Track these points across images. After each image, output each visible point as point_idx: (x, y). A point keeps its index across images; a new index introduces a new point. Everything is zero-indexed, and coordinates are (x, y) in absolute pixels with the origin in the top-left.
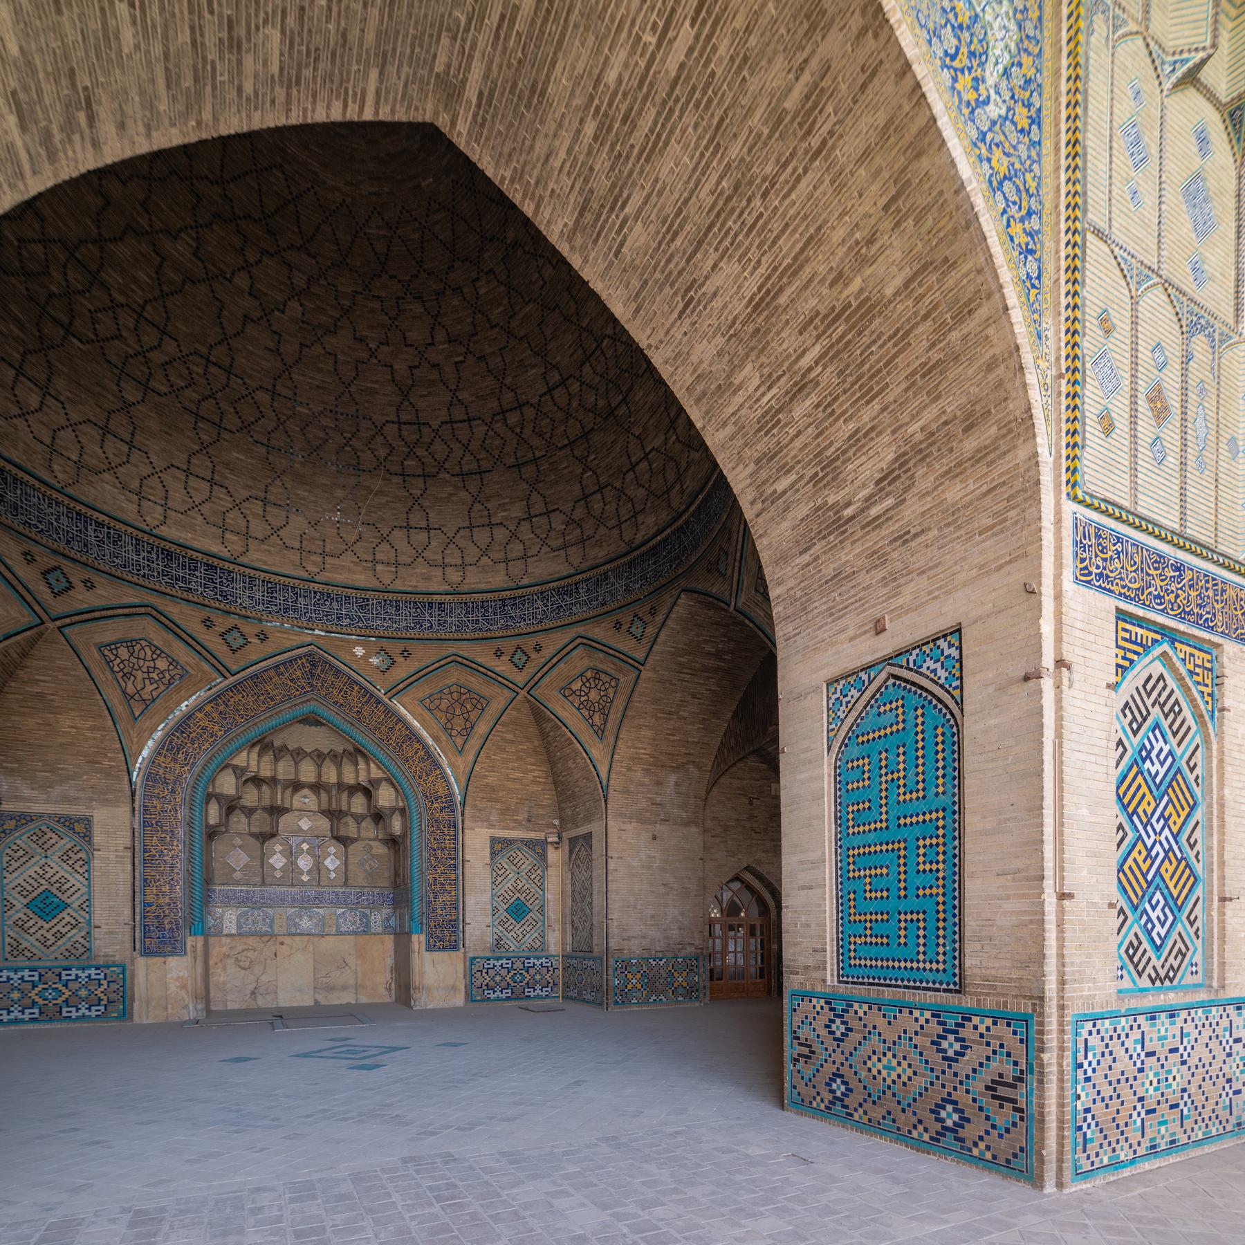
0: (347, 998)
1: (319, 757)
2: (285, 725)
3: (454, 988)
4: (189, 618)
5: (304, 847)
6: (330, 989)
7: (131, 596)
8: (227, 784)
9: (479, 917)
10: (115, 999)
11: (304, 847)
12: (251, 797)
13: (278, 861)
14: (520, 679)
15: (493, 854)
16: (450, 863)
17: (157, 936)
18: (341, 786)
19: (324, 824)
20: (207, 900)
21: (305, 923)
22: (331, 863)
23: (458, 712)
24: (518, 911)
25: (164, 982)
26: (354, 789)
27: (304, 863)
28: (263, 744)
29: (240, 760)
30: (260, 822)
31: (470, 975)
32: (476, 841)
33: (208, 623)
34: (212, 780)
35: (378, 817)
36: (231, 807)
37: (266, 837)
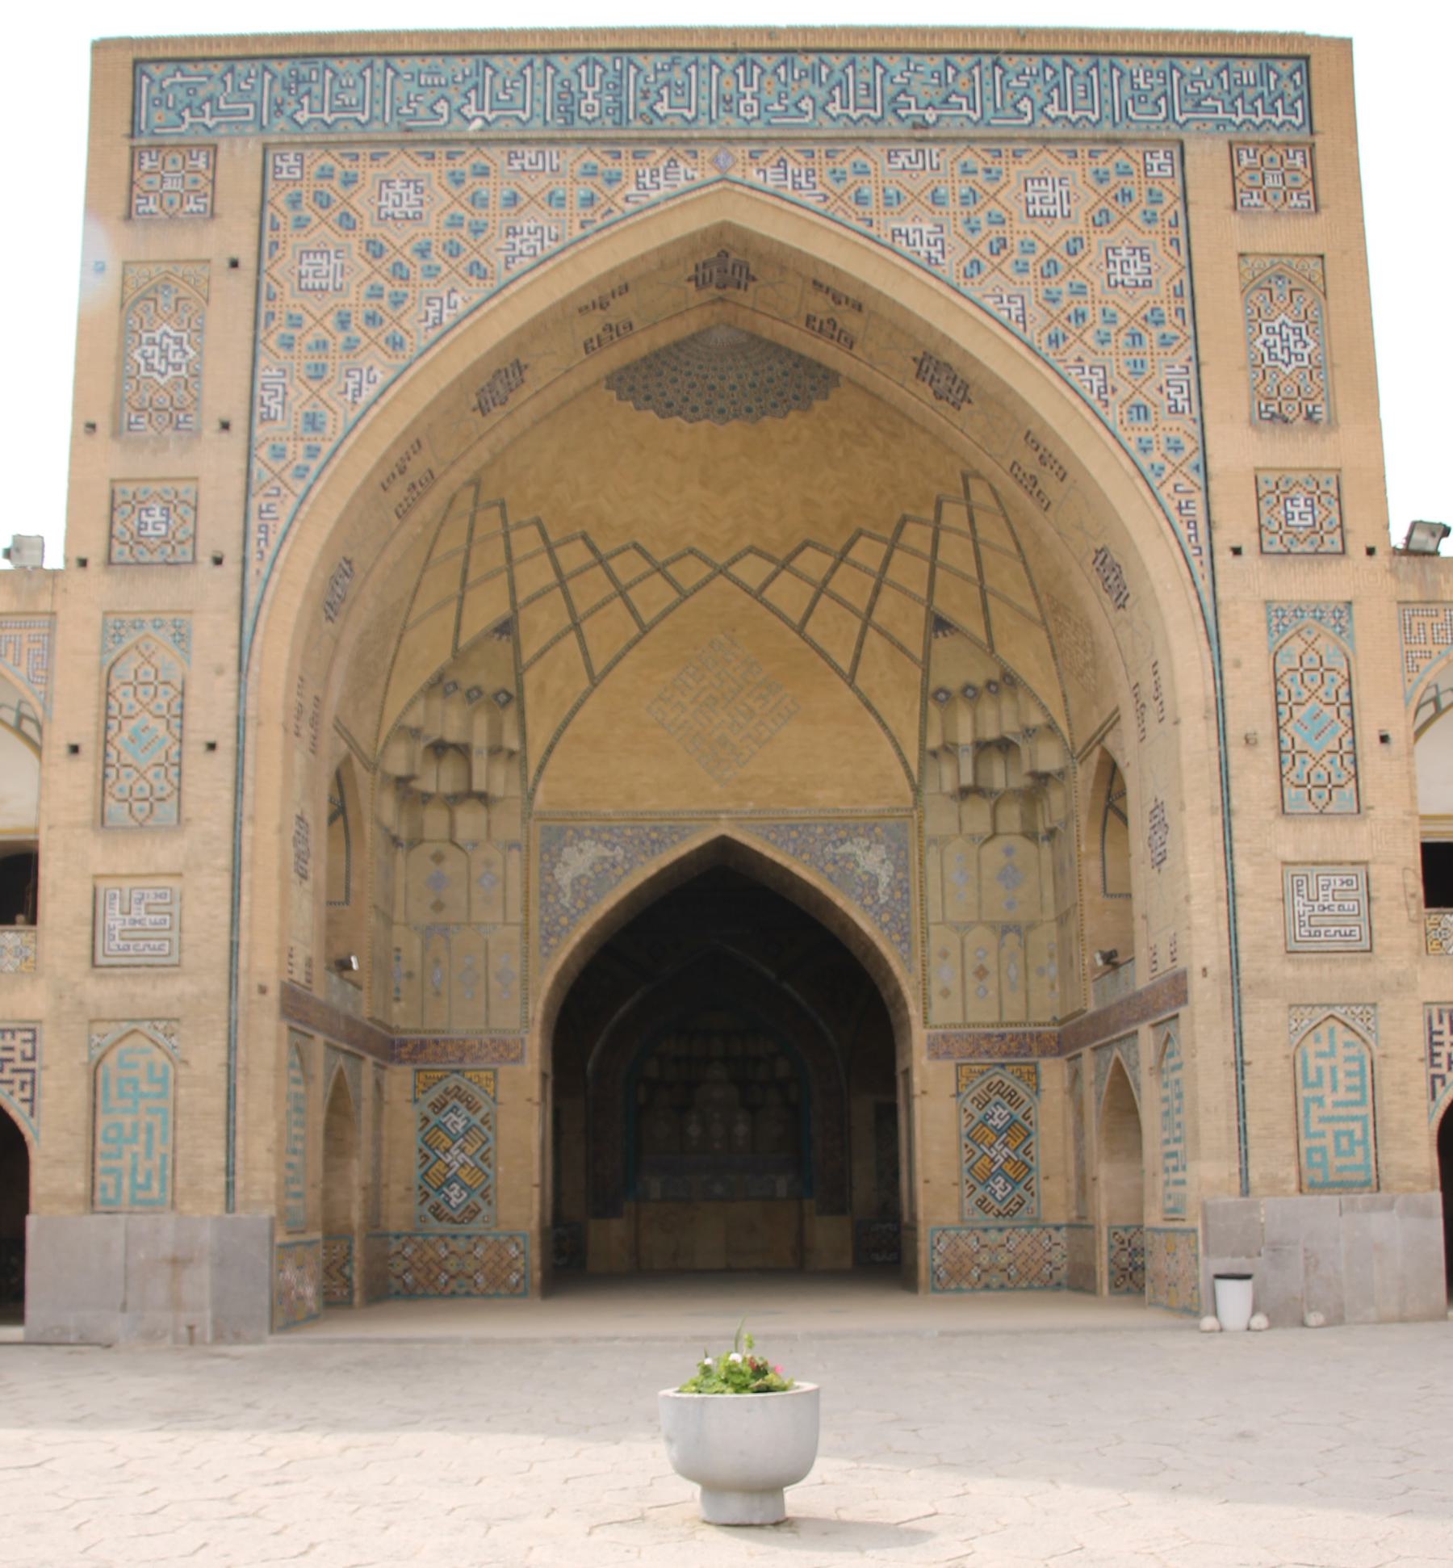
13: (694, 1130)
21: (718, 1189)
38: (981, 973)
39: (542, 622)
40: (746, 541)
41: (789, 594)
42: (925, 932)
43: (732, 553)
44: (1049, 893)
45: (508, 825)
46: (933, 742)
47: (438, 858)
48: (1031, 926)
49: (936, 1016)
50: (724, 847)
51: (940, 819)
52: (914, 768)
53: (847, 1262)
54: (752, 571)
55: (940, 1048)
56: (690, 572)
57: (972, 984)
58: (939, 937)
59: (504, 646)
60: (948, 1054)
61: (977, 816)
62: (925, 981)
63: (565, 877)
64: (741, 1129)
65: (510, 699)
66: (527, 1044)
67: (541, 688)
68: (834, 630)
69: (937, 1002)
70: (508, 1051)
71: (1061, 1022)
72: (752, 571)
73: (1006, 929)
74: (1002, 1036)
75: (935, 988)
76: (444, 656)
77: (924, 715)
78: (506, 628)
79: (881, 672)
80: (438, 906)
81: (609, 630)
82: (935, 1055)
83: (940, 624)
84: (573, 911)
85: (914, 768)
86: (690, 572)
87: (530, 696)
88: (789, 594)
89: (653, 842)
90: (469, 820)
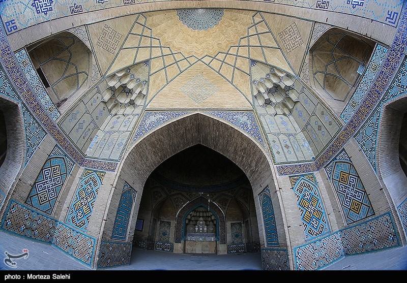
0: (207, 252)
1: (203, 212)
2: (197, 208)
3: (225, 251)
4: (185, 194)
5: (201, 226)
6: (204, 251)
7: (175, 192)
8: (189, 217)
9: (229, 238)
10: (172, 249)
11: (201, 226)
12: (193, 219)
14: (233, 196)
15: (231, 226)
16: (224, 229)
17: (178, 241)
18: (206, 216)
19: (204, 222)
20: (185, 235)
21: (201, 239)
22: (205, 229)
23: (223, 202)
24: (237, 236)
25: (178, 247)
26: (209, 216)
27: (201, 229)
28: (194, 211)
29: (191, 214)
30: (194, 223)
31: (228, 248)
32: (228, 224)
33: (187, 194)
34: (187, 216)
35: (212, 221)
36: (190, 220)
37: (195, 225)
38: (287, 147)
39: (156, 65)
40: (205, 54)
41: (215, 64)
42: (266, 136)
43: (203, 56)
44: (296, 126)
45: (138, 111)
46: (255, 94)
47: (118, 118)
48: (295, 134)
49: (278, 161)
50: (198, 122)
51: (260, 111)
52: (251, 101)
53: (226, 253)
54: (207, 60)
55: (282, 171)
56: (193, 60)
57: (286, 150)
58: (270, 137)
59: (147, 68)
60: (285, 174)
61: (271, 110)
62: (270, 149)
63: (148, 122)
64: (205, 229)
65: (147, 82)
66: (118, 165)
67: (154, 81)
68: (227, 71)
69: (276, 155)
70: (111, 167)
71: (317, 157)
72: (207, 60)
73: (290, 135)
74: (300, 165)
75: (274, 151)
76: (131, 63)
77: (252, 87)
78: (146, 62)
79: (238, 79)
80: (113, 127)
81: (172, 71)
82: (281, 174)
83: (254, 62)
84: (147, 129)
85: (251, 101)
86: (193, 60)
87: (151, 82)
88: (215, 64)
89: (176, 115)
90: (129, 110)
